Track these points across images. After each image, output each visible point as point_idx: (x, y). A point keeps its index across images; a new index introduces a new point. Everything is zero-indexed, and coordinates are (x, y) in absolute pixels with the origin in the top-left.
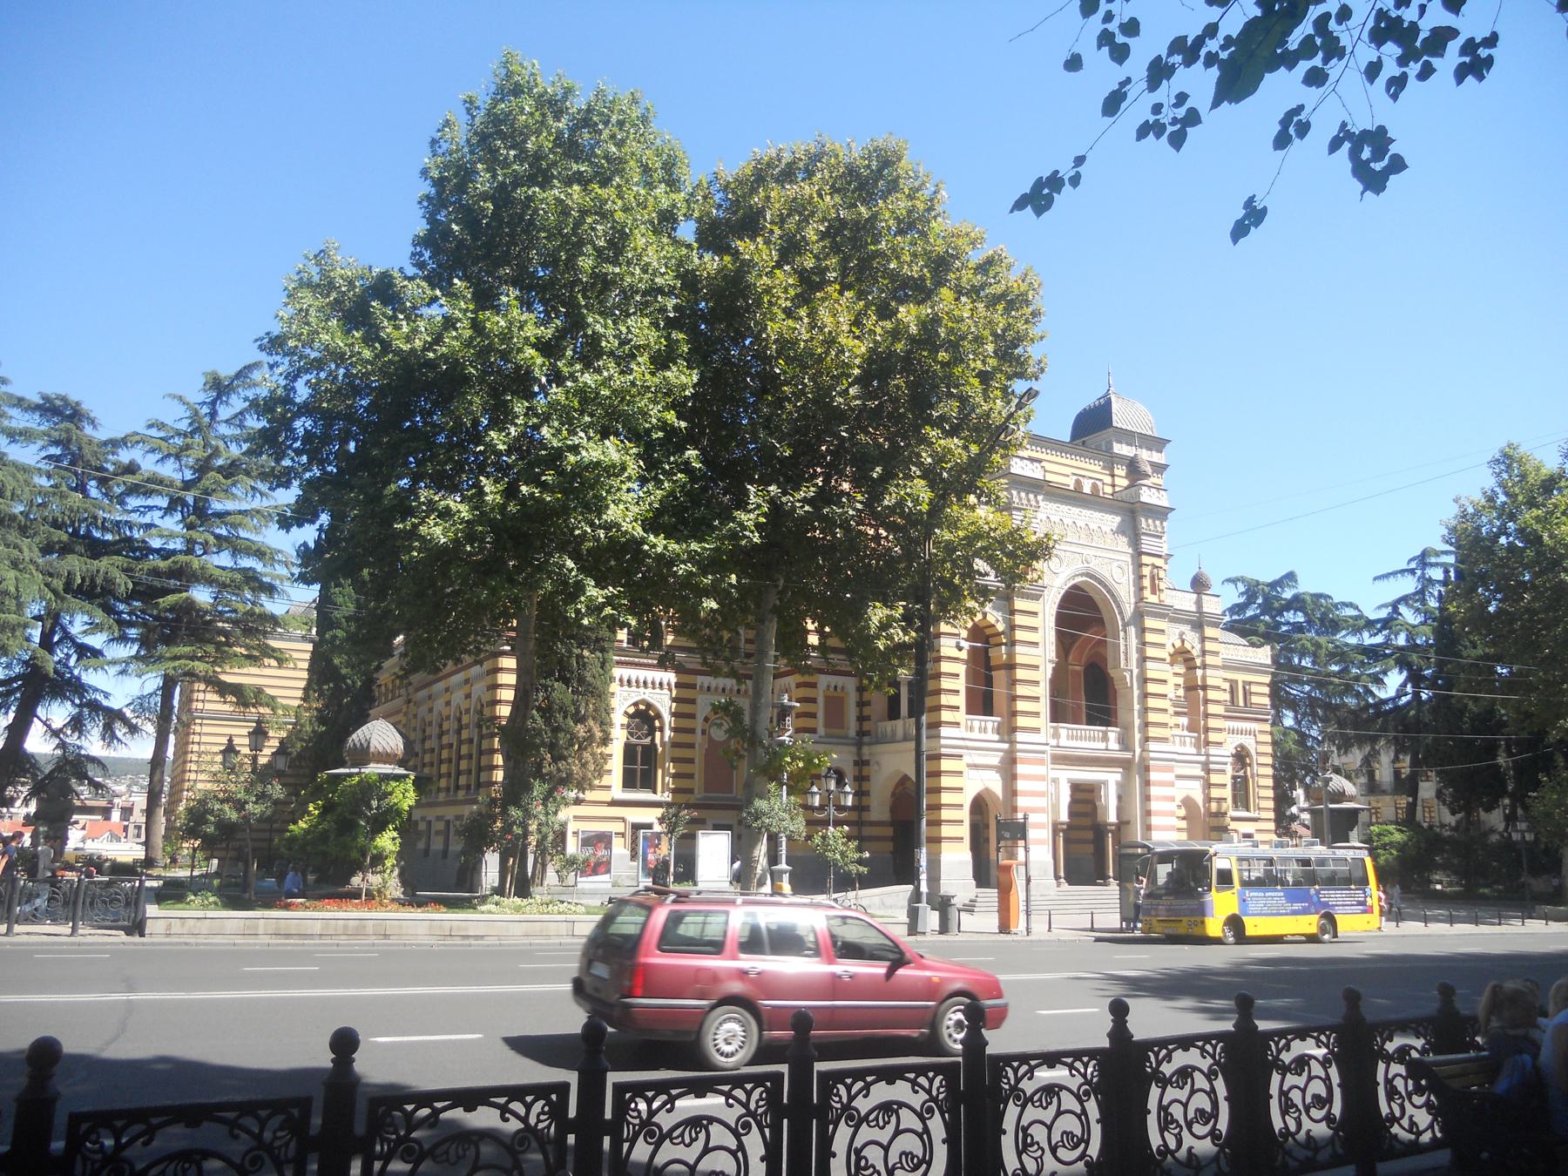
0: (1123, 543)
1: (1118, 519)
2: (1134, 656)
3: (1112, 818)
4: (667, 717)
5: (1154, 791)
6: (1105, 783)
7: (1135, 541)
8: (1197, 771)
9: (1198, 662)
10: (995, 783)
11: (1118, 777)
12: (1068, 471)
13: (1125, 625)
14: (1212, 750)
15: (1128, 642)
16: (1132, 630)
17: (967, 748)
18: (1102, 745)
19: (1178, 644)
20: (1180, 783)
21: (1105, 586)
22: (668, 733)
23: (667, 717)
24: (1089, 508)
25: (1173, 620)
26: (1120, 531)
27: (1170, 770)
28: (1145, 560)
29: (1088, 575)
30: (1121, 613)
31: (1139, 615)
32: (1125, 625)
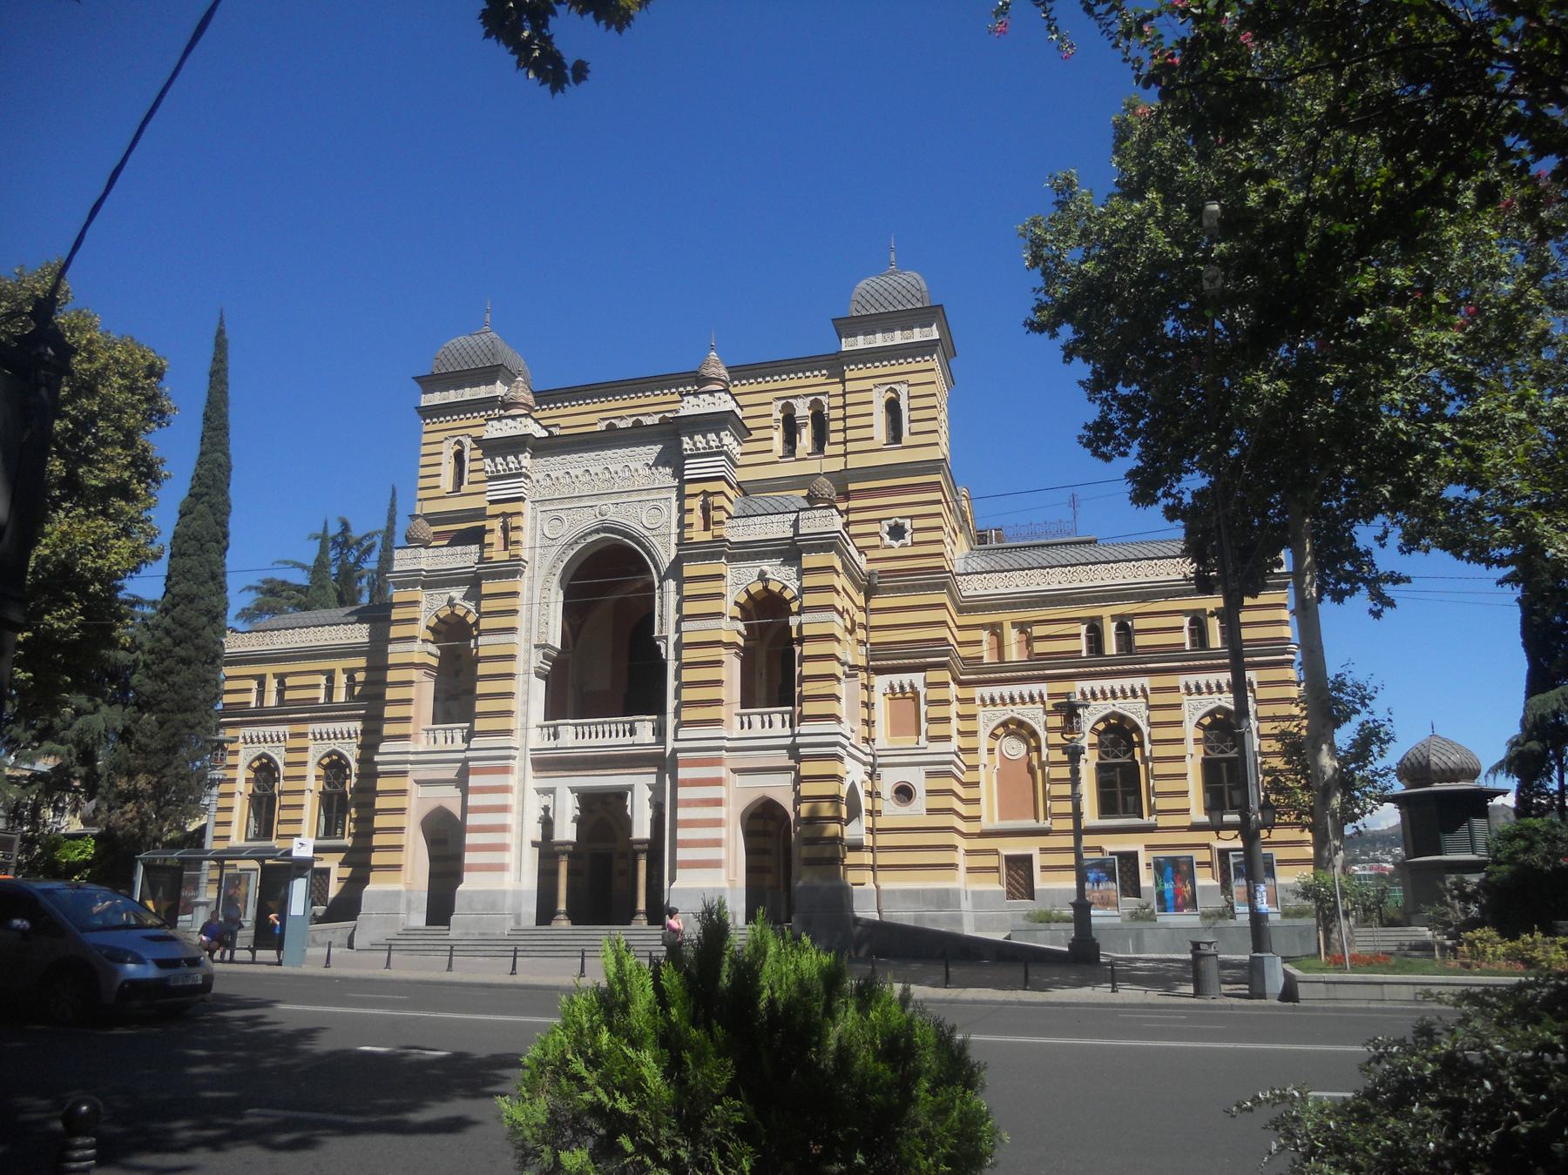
0: (665, 476)
1: (658, 448)
2: (672, 617)
3: (642, 829)
4: (354, 766)
5: (683, 793)
6: (631, 788)
7: (678, 473)
8: (782, 759)
9: (794, 607)
10: (449, 798)
11: (652, 779)
12: (768, 397)
13: (662, 580)
14: (804, 728)
15: (667, 600)
16: (671, 585)
17: (412, 763)
18: (628, 740)
19: (756, 588)
20: (739, 780)
21: (632, 538)
22: (354, 780)
23: (354, 766)
24: (592, 450)
25: (732, 558)
26: (661, 461)
27: (717, 762)
28: (689, 489)
29: (605, 530)
30: (656, 567)
31: (675, 570)
32: (662, 580)
